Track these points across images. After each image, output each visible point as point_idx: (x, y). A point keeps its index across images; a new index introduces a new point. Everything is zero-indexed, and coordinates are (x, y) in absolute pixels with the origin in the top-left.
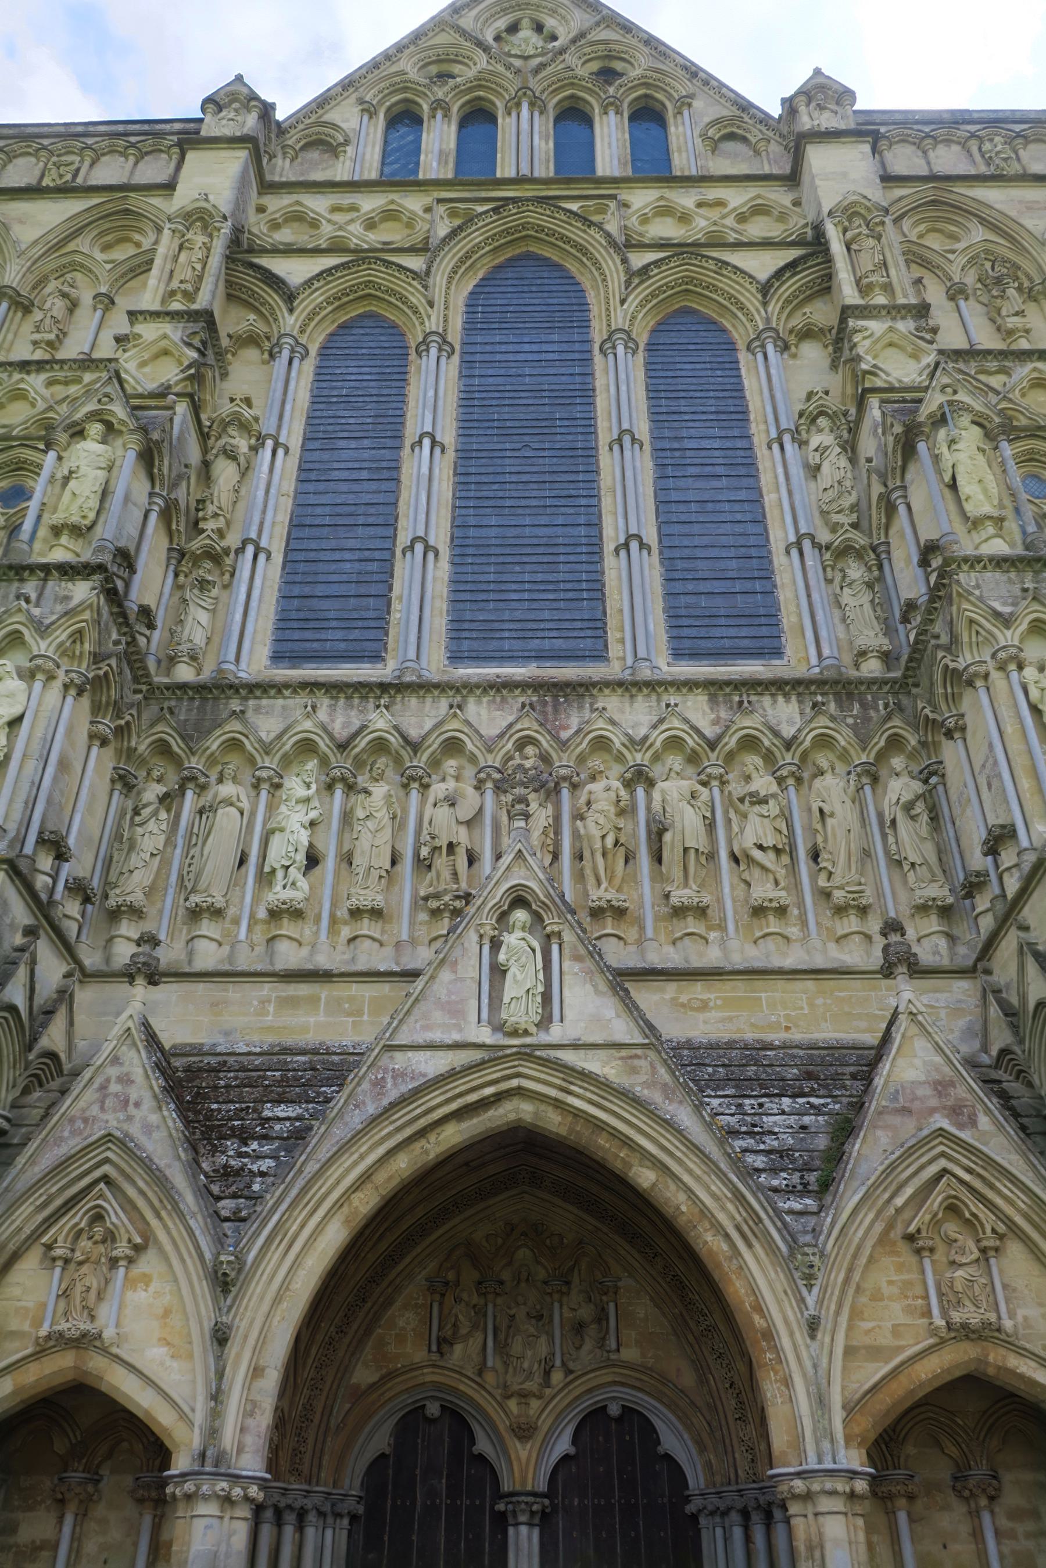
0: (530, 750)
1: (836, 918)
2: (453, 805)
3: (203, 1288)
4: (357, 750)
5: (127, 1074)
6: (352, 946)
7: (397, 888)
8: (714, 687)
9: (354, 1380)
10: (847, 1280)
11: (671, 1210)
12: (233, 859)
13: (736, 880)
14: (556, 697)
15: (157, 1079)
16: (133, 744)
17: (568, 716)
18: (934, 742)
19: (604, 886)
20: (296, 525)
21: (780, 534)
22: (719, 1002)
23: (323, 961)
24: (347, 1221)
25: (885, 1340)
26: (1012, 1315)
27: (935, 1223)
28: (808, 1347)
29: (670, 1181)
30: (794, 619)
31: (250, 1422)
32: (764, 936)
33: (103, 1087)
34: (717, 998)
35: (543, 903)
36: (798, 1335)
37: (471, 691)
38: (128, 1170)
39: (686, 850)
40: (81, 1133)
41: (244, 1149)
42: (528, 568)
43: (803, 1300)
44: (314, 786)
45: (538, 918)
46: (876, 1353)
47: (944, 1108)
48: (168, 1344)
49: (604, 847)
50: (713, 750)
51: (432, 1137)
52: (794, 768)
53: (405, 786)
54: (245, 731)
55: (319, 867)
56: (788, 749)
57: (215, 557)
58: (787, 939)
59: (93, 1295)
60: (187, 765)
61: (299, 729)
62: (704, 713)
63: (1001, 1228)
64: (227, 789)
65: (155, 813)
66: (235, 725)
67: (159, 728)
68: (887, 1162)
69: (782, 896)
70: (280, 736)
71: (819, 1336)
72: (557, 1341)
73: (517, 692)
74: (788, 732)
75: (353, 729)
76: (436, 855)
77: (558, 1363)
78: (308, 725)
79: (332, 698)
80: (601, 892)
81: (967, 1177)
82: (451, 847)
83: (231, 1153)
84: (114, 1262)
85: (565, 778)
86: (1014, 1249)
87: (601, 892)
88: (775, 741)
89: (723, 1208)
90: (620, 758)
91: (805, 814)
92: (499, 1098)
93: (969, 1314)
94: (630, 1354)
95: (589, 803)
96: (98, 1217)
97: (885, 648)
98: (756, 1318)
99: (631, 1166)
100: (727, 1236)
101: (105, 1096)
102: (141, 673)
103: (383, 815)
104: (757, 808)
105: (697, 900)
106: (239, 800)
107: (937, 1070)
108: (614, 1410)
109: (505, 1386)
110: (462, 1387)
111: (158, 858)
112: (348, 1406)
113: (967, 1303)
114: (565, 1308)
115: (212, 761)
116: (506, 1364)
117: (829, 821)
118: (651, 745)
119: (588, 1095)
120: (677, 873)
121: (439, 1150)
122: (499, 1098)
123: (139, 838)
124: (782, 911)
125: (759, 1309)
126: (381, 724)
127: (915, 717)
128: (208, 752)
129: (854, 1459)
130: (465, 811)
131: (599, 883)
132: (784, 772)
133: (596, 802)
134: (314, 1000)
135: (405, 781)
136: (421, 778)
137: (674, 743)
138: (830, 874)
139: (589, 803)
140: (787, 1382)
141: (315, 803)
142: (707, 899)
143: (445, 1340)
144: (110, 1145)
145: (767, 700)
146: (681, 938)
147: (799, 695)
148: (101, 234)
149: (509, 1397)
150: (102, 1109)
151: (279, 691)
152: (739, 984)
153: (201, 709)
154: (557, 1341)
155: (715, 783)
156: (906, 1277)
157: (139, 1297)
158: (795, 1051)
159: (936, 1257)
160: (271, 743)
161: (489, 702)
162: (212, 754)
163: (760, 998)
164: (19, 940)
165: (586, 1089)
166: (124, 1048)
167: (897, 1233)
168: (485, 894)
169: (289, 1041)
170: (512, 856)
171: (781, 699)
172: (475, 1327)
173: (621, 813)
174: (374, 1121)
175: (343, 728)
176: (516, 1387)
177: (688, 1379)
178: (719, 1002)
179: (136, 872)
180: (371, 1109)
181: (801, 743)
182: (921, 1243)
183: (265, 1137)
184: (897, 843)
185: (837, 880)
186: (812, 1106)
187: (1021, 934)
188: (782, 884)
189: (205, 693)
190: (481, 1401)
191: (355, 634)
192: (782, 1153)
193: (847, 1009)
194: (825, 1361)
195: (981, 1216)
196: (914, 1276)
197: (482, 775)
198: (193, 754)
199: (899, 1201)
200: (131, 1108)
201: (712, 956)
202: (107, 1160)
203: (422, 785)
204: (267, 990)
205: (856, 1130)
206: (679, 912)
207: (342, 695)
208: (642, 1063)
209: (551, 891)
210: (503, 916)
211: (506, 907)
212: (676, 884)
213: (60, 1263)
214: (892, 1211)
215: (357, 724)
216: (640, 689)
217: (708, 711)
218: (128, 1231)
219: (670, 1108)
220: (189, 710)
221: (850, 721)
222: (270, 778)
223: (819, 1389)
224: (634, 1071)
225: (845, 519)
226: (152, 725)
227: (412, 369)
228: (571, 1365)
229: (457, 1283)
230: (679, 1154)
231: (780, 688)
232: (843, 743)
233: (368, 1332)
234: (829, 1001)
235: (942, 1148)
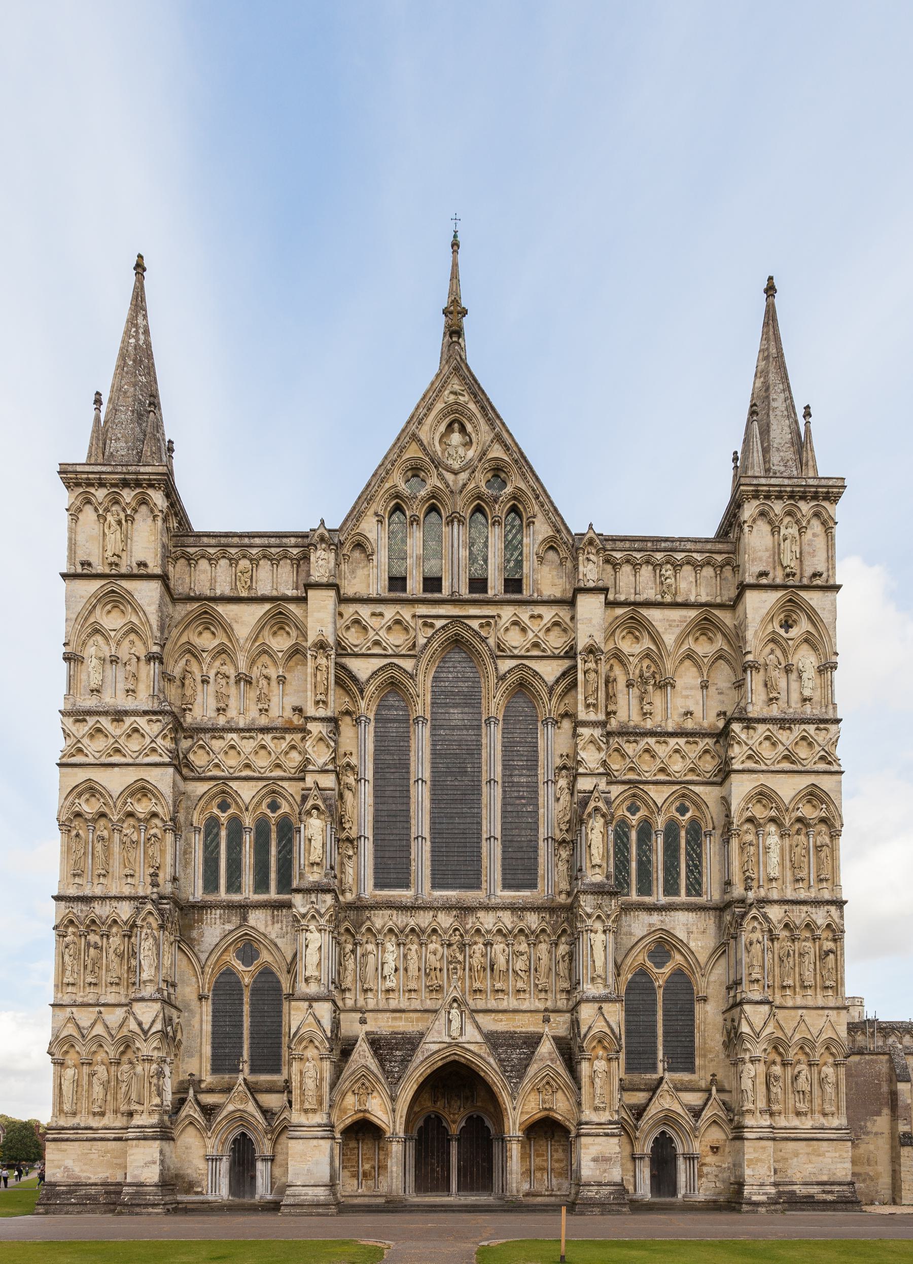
0: (457, 933)
3: (388, 1100)
8: (513, 908)
20: (376, 821)
21: (542, 833)
25: (530, 1110)
27: (544, 1086)
42: (457, 845)
46: (527, 1113)
57: (349, 840)
67: (347, 923)
70: (383, 927)
74: (534, 927)
75: (404, 924)
78: (391, 923)
86: (560, 1092)
93: (547, 1106)
96: (363, 1084)
126: (413, 923)
129: (520, 1134)
130: (438, 956)
137: (499, 931)
145: (528, 913)
148: (272, 627)
153: (357, 915)
157: (374, 1101)
225: (564, 828)
227: (412, 729)
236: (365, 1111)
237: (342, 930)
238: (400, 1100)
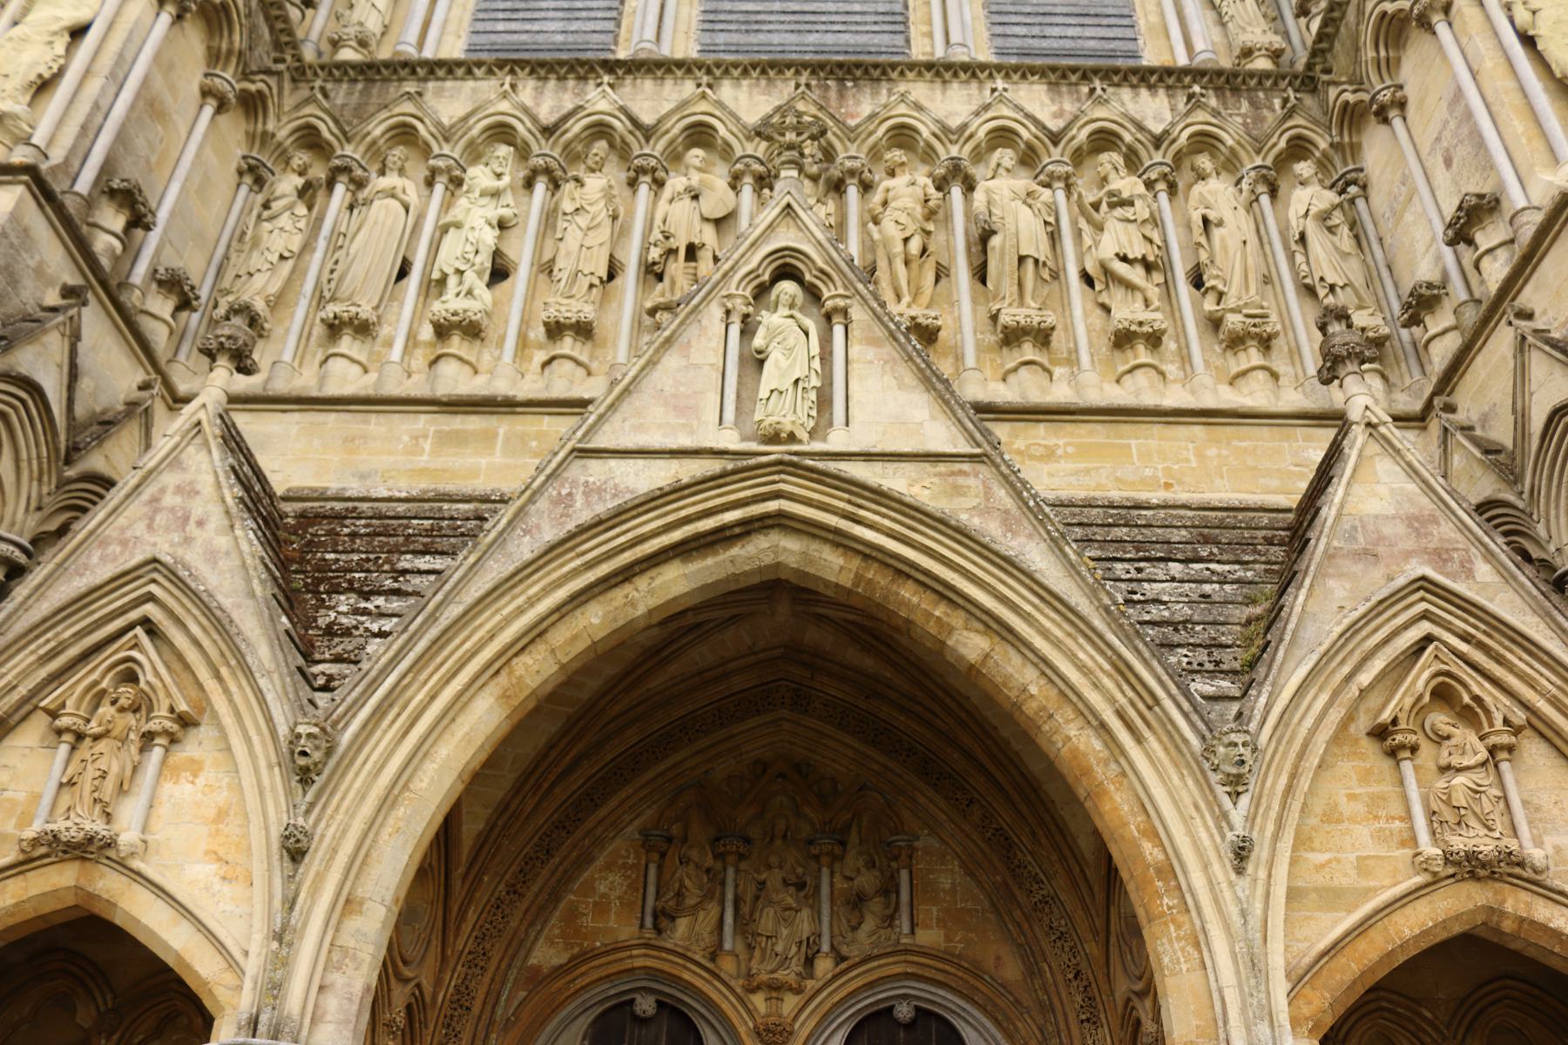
1: (1229, 354)
2: (695, 197)
3: (274, 780)
4: (569, 135)
5: (191, 483)
6: (547, 371)
7: (614, 305)
9: (533, 961)
10: (1289, 790)
11: (1013, 694)
12: (391, 266)
13: (1090, 305)
14: (841, 80)
15: (231, 487)
16: (270, 126)
17: (858, 103)
18: (1352, 145)
19: (906, 299)
22: (1070, 450)
23: (502, 387)
24: (505, 696)
25: (1346, 878)
26: (1538, 843)
27: (1419, 709)
28: (1231, 885)
29: (1012, 652)
30: (1154, 19)
31: (336, 978)
32: (1130, 371)
33: (155, 500)
34: (1067, 444)
35: (822, 271)
36: (1216, 867)
37: (727, 72)
38: (178, 610)
39: (1022, 259)
40: (115, 559)
41: (363, 605)
43: (1225, 816)
44: (506, 179)
45: (813, 294)
46: (1333, 897)
47: (1425, 551)
48: (219, 859)
49: (906, 253)
50: (1055, 144)
51: (642, 583)
52: (1167, 170)
53: (633, 184)
54: (420, 114)
55: (510, 280)
56: (1157, 147)
58: (1162, 374)
59: (109, 785)
60: (339, 152)
61: (491, 110)
62: (1042, 105)
63: (1519, 716)
64: (391, 180)
65: (290, 207)
66: (408, 107)
68: (1347, 622)
69: (1157, 319)
71: (1250, 868)
72: (826, 919)
73: (789, 73)
74: (1157, 129)
76: (671, 259)
77: (825, 947)
78: (504, 106)
79: (539, 79)
80: (902, 307)
81: (1463, 647)
82: (692, 252)
83: (343, 608)
84: (148, 738)
85: (852, 173)
87: (902, 307)
88: (1139, 136)
89: (1097, 686)
90: (929, 155)
91: (1181, 230)
92: (749, 528)
94: (929, 937)
95: (885, 203)
97: (1276, 46)
98: (1147, 847)
99: (951, 630)
100: (1103, 726)
101: (156, 511)
102: (285, 39)
103: (600, 211)
104: (1119, 212)
105: (1037, 319)
106: (404, 191)
107: (1411, 501)
108: (904, 1012)
109: (749, 975)
110: (686, 976)
111: (290, 263)
112: (523, 994)
113: (1473, 822)
114: (837, 879)
115: (373, 149)
116: (750, 948)
117: (1217, 233)
118: (971, 136)
119: (887, 522)
120: (1009, 288)
121: (653, 602)
122: (749, 528)
123: (265, 236)
124: (1154, 340)
125: (1153, 835)
126: (603, 105)
127: (1326, 113)
128: (369, 139)
131: (899, 298)
132: (1153, 176)
133: (895, 199)
134: (489, 438)
135: (632, 174)
136: (654, 170)
137: (1002, 136)
138: (1221, 295)
139: (885, 203)
140: (1199, 940)
141: (508, 198)
142: (1050, 319)
143: (664, 913)
144: (156, 576)
146: (1015, 370)
147: (1168, 88)
149: (753, 991)
150: (150, 527)
151: (469, 72)
152: (1099, 427)
153: (365, 93)
154: (826, 919)
155: (1059, 185)
156: (1376, 789)
157: (180, 791)
158: (1182, 512)
159: (1418, 761)
160: (452, 126)
161: (750, 86)
162: (374, 142)
163: (1129, 447)
164: (52, 298)
165: (884, 516)
166: (191, 449)
167: (1363, 723)
168: (736, 256)
169: (450, 487)
170: (778, 210)
171: (1144, 92)
172: (708, 896)
173: (930, 215)
174: (553, 551)
175: (551, 113)
176: (764, 977)
177: (1012, 971)
178: (1070, 450)
179: (257, 276)
180: (550, 534)
181: (1174, 141)
182: (1399, 738)
183: (397, 592)
184: (1308, 263)
185: (1230, 302)
186: (1213, 572)
187: (1523, 324)
188: (1156, 303)
189: (370, 73)
190: (714, 996)
191: (574, 26)
192: (1175, 625)
193: (1250, 462)
194: (1258, 907)
195: (1488, 699)
196: (1387, 788)
197: (738, 166)
198: (348, 140)
199: (1365, 678)
200: (191, 527)
201: (1060, 393)
202: (150, 598)
203: (655, 181)
204: (423, 422)
205: (1299, 577)
206: (1012, 337)
207: (553, 76)
208: (971, 481)
209: (835, 255)
210: (761, 292)
211: (766, 277)
212: (1007, 301)
213: (68, 737)
214: (1354, 691)
215: (569, 106)
216: (956, 75)
217: (1046, 100)
218: (169, 695)
219: (1014, 543)
220: (349, 94)
221: (1239, 120)
222: (449, 170)
223: (1250, 948)
224: (958, 491)
226: (298, 107)
228: (844, 950)
229: (685, 840)
230: (1028, 608)
231: (1143, 79)
232: (1230, 142)
233: (555, 897)
234: (1225, 453)
235: (1424, 606)
236: (88, 850)
237: (282, 129)
238: (354, 781)
